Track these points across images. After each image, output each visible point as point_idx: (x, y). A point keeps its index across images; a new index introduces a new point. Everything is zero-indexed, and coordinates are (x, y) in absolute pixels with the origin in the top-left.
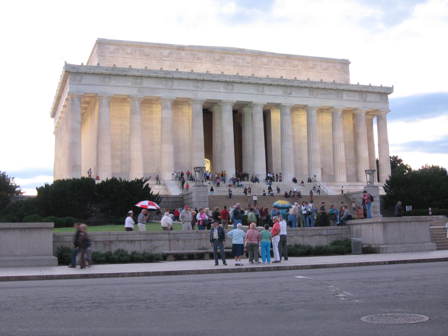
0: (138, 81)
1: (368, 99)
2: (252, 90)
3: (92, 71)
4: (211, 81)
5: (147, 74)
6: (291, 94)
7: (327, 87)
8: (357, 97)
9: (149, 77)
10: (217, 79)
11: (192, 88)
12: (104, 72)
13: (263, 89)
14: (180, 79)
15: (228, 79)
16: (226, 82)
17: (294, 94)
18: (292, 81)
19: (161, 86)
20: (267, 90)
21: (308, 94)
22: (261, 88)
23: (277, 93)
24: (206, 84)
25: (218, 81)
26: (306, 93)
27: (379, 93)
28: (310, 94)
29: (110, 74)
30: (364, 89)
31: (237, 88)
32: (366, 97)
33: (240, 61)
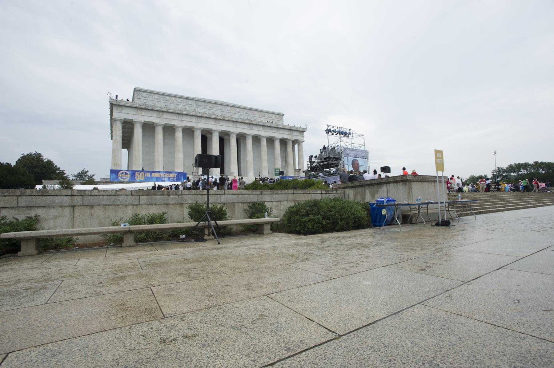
0: (161, 114)
2: (230, 124)
4: (206, 117)
5: (166, 110)
8: (288, 132)
9: (168, 112)
10: (209, 116)
12: (138, 106)
14: (187, 115)
15: (216, 117)
16: (215, 119)
19: (175, 118)
20: (238, 125)
22: (235, 124)
25: (210, 118)
26: (261, 128)
27: (299, 131)
29: (142, 109)
30: (292, 129)
31: (221, 123)
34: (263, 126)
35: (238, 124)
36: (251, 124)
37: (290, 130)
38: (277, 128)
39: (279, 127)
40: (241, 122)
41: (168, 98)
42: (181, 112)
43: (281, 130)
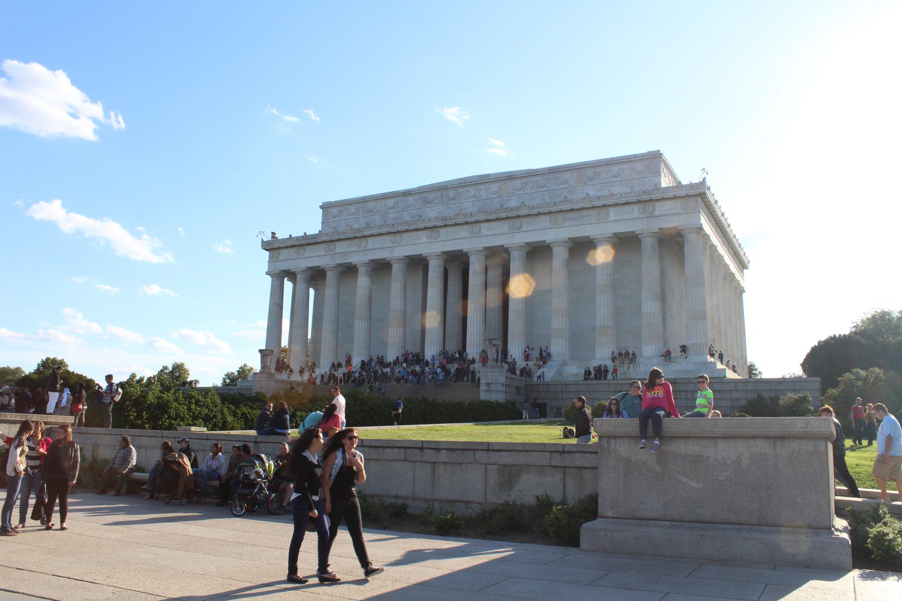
0: (331, 245)
1: (657, 213)
2: (463, 231)
3: (284, 245)
4: (408, 231)
6: (521, 227)
7: (575, 207)
8: (635, 211)
9: (339, 240)
11: (388, 245)
12: (295, 243)
13: (480, 228)
14: (372, 235)
15: (428, 225)
16: (426, 228)
17: (525, 228)
18: (518, 208)
20: (485, 228)
21: (548, 224)
22: (476, 227)
23: (499, 231)
24: (404, 235)
25: (416, 230)
28: (551, 221)
32: (654, 209)
33: (483, 192)
34: (550, 213)
35: (484, 226)
36: (514, 217)
37: (639, 202)
38: (594, 207)
39: (595, 203)
40: (487, 221)
41: (371, 205)
42: (360, 235)
43: (612, 211)
